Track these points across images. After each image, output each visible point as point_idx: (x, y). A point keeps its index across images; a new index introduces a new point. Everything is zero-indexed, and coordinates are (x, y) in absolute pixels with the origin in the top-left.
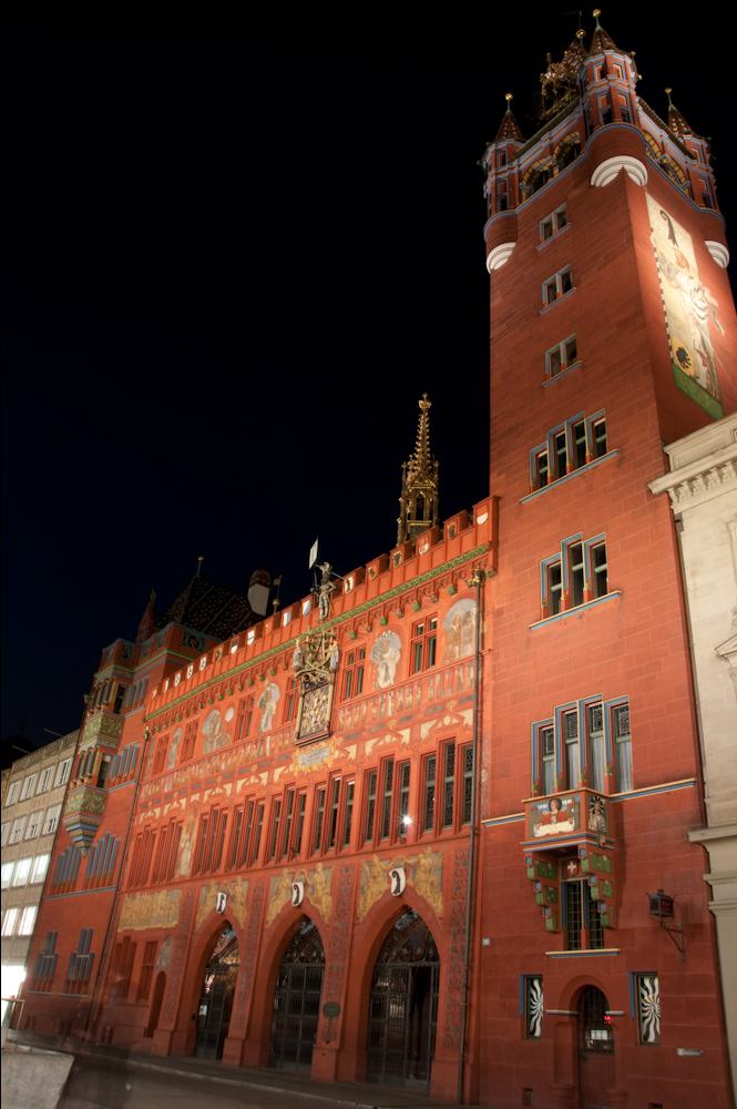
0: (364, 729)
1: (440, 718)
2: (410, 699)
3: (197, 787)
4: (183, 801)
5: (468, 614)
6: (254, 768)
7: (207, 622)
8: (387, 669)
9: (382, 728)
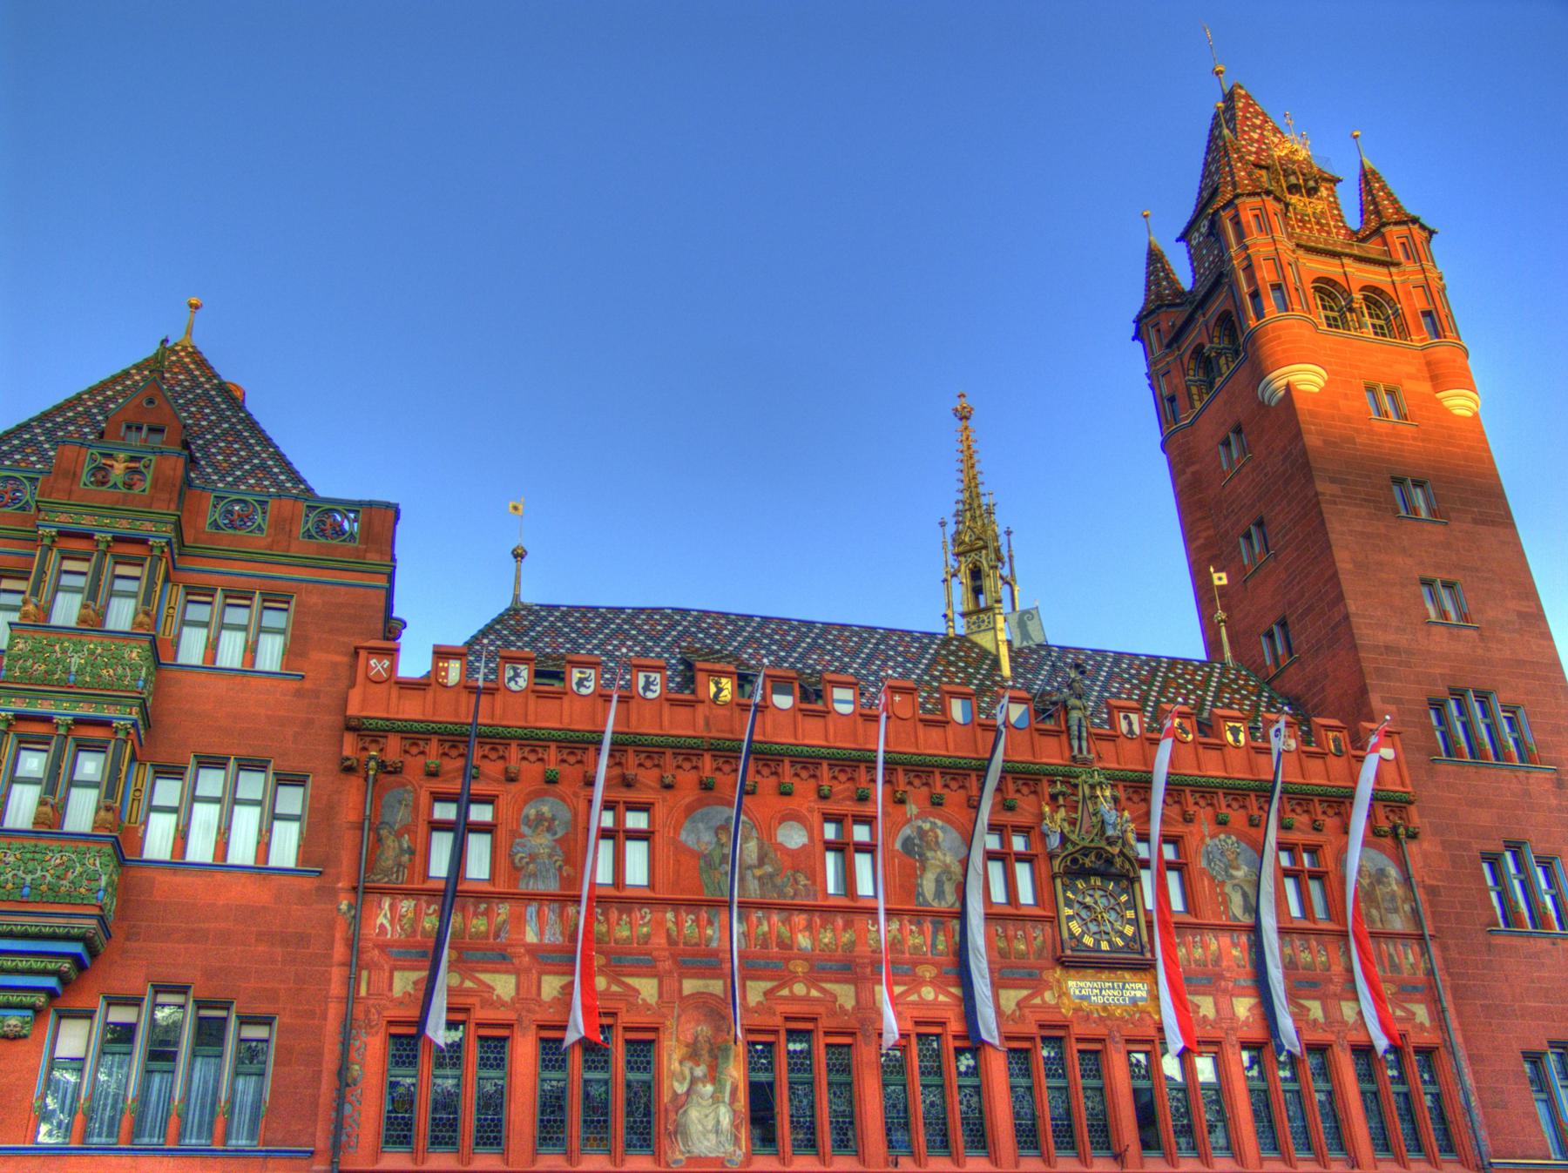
0: (1220, 977)
2: (1306, 957)
4: (647, 988)
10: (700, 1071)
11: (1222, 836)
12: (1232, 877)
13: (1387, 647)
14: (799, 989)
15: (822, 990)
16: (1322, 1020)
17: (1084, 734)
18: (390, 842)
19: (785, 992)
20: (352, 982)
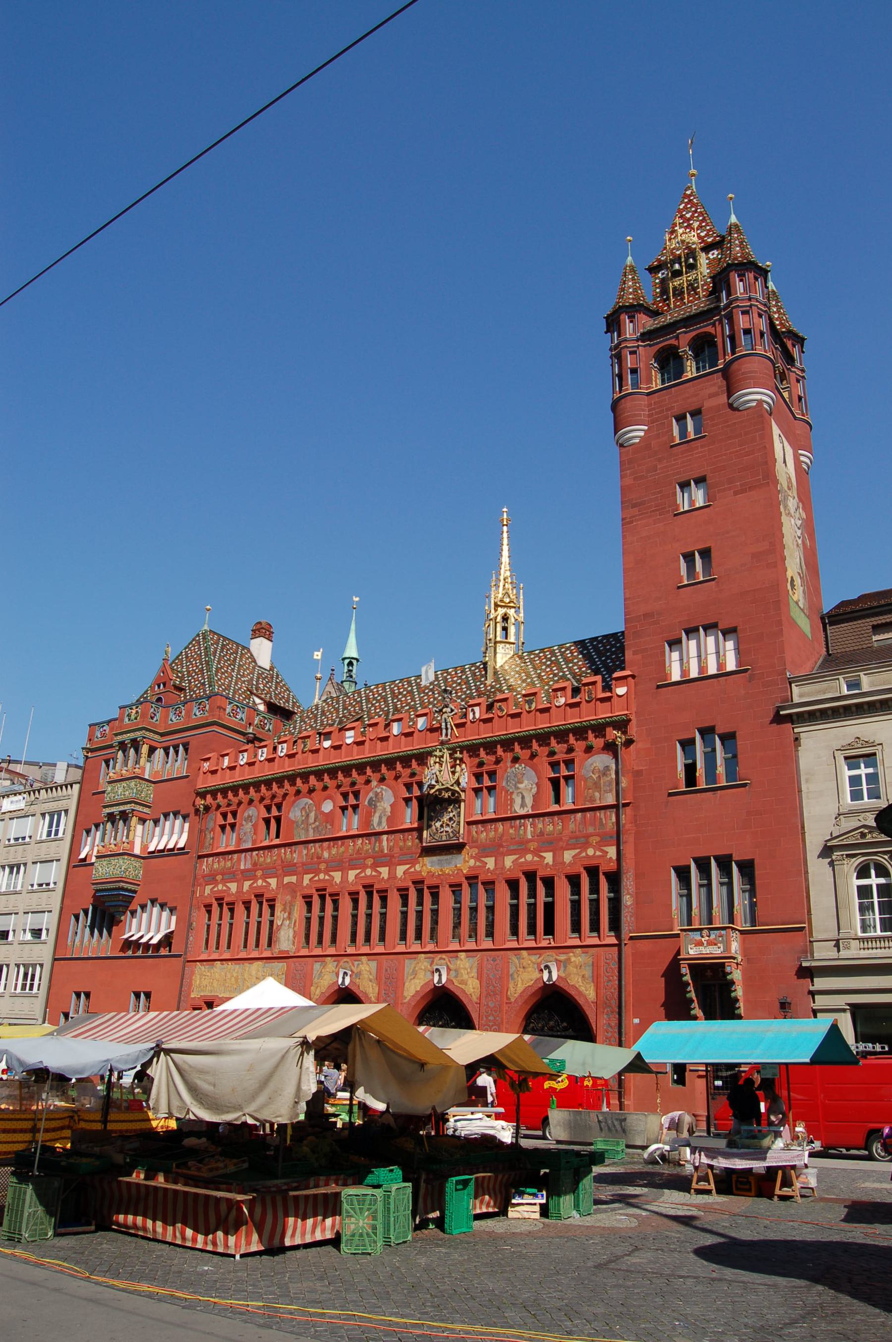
0: (501, 846)
1: (585, 850)
2: (550, 828)
3: (289, 868)
4: (273, 882)
5: (607, 768)
6: (370, 862)
7: (230, 682)
8: (523, 798)
9: (522, 847)
10: (286, 915)
11: (517, 766)
12: (518, 788)
13: (646, 615)
14: (322, 876)
15: (329, 875)
16: (551, 863)
17: (449, 726)
18: (208, 836)
19: (316, 878)
20: (194, 892)
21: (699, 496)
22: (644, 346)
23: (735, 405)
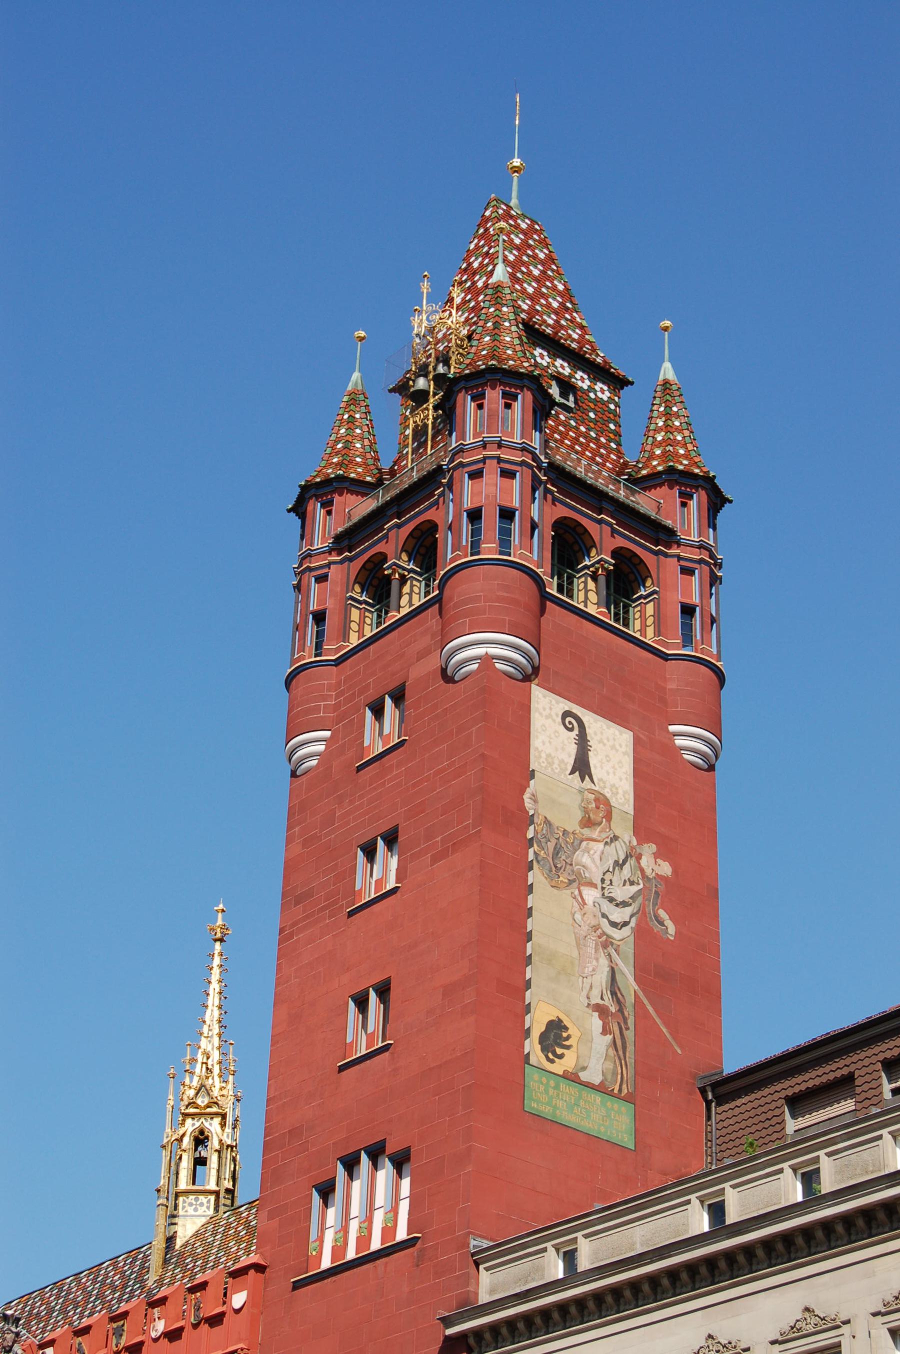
21: (387, 868)
22: (341, 562)
23: (449, 672)
